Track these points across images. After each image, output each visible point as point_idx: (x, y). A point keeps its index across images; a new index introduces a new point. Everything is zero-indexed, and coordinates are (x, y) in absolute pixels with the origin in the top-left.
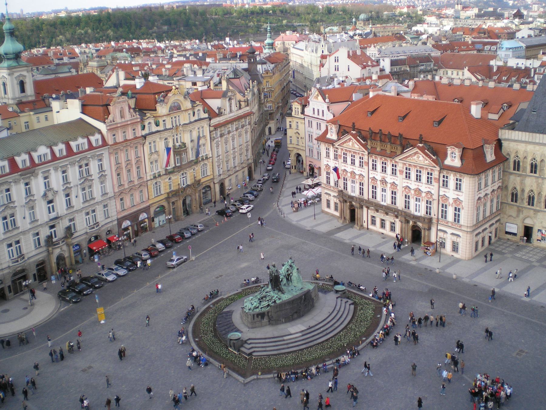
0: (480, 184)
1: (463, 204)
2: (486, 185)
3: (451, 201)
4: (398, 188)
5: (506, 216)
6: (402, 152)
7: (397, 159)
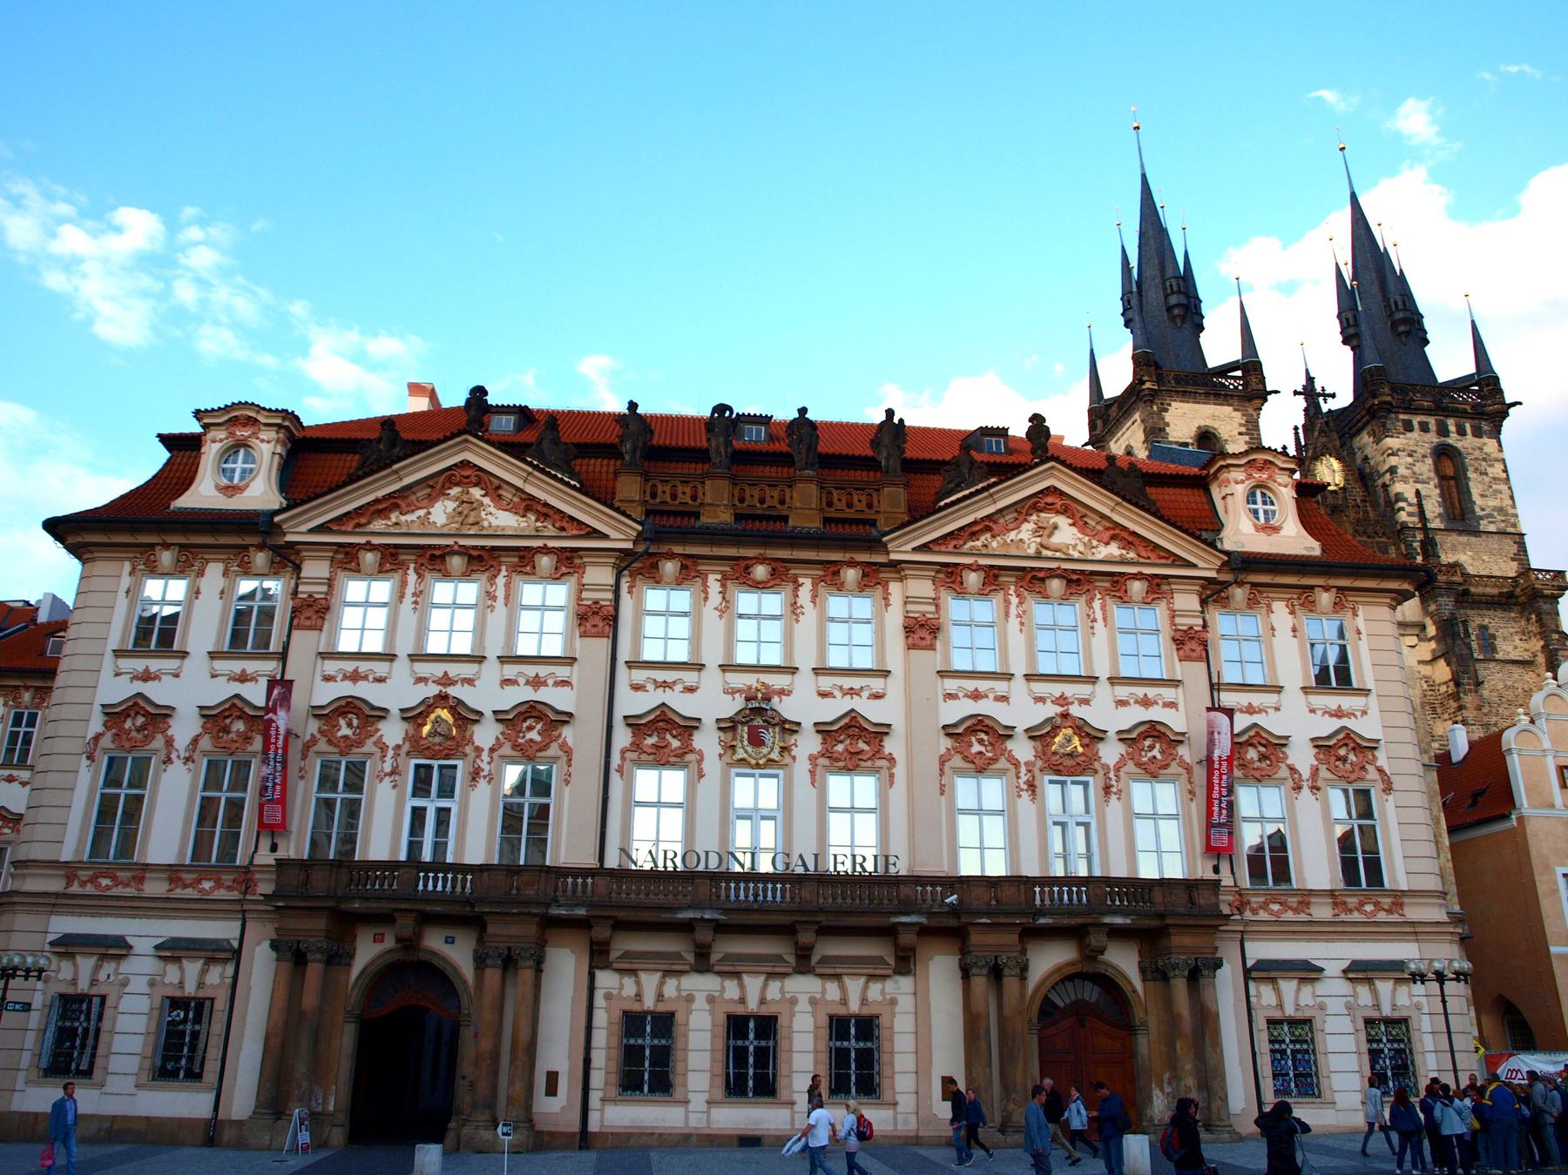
1: (1382, 761)
3: (1301, 757)
4: (891, 746)
7: (902, 548)
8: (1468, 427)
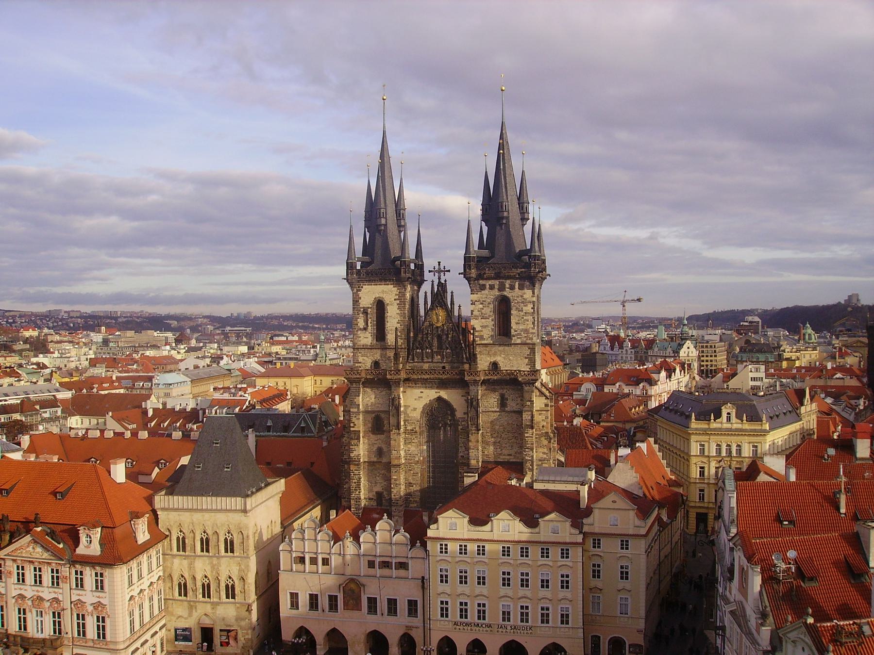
0: (130, 577)
2: (140, 577)
5: (174, 619)
6: (10, 543)
8: (517, 284)
